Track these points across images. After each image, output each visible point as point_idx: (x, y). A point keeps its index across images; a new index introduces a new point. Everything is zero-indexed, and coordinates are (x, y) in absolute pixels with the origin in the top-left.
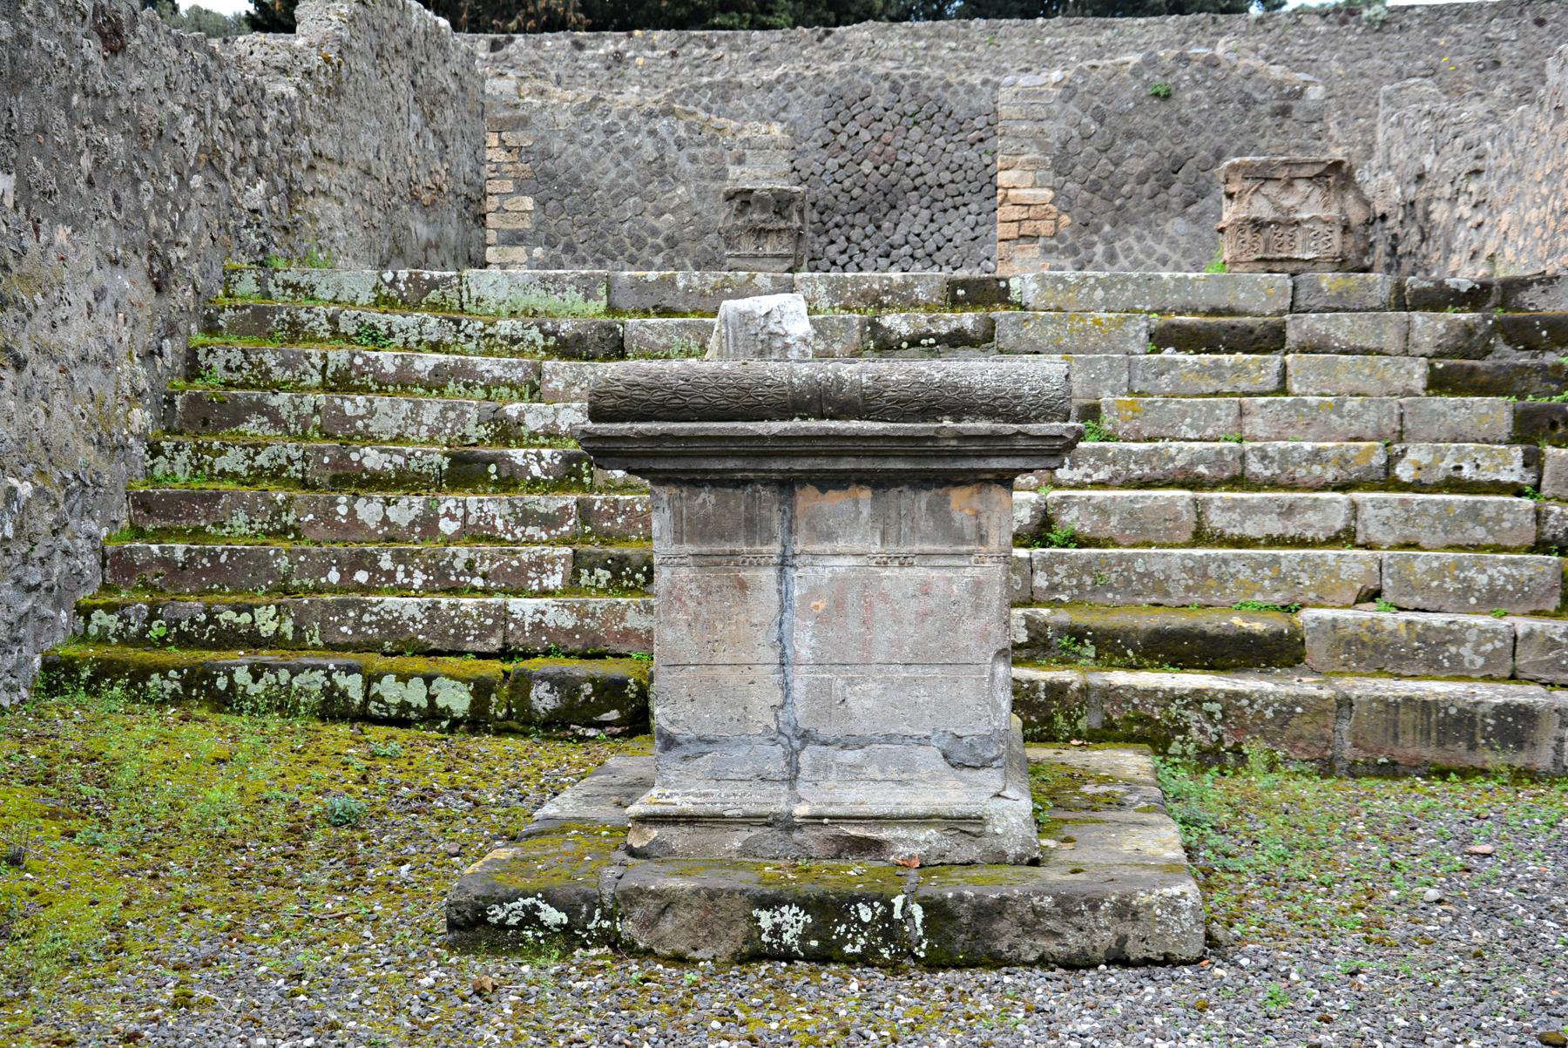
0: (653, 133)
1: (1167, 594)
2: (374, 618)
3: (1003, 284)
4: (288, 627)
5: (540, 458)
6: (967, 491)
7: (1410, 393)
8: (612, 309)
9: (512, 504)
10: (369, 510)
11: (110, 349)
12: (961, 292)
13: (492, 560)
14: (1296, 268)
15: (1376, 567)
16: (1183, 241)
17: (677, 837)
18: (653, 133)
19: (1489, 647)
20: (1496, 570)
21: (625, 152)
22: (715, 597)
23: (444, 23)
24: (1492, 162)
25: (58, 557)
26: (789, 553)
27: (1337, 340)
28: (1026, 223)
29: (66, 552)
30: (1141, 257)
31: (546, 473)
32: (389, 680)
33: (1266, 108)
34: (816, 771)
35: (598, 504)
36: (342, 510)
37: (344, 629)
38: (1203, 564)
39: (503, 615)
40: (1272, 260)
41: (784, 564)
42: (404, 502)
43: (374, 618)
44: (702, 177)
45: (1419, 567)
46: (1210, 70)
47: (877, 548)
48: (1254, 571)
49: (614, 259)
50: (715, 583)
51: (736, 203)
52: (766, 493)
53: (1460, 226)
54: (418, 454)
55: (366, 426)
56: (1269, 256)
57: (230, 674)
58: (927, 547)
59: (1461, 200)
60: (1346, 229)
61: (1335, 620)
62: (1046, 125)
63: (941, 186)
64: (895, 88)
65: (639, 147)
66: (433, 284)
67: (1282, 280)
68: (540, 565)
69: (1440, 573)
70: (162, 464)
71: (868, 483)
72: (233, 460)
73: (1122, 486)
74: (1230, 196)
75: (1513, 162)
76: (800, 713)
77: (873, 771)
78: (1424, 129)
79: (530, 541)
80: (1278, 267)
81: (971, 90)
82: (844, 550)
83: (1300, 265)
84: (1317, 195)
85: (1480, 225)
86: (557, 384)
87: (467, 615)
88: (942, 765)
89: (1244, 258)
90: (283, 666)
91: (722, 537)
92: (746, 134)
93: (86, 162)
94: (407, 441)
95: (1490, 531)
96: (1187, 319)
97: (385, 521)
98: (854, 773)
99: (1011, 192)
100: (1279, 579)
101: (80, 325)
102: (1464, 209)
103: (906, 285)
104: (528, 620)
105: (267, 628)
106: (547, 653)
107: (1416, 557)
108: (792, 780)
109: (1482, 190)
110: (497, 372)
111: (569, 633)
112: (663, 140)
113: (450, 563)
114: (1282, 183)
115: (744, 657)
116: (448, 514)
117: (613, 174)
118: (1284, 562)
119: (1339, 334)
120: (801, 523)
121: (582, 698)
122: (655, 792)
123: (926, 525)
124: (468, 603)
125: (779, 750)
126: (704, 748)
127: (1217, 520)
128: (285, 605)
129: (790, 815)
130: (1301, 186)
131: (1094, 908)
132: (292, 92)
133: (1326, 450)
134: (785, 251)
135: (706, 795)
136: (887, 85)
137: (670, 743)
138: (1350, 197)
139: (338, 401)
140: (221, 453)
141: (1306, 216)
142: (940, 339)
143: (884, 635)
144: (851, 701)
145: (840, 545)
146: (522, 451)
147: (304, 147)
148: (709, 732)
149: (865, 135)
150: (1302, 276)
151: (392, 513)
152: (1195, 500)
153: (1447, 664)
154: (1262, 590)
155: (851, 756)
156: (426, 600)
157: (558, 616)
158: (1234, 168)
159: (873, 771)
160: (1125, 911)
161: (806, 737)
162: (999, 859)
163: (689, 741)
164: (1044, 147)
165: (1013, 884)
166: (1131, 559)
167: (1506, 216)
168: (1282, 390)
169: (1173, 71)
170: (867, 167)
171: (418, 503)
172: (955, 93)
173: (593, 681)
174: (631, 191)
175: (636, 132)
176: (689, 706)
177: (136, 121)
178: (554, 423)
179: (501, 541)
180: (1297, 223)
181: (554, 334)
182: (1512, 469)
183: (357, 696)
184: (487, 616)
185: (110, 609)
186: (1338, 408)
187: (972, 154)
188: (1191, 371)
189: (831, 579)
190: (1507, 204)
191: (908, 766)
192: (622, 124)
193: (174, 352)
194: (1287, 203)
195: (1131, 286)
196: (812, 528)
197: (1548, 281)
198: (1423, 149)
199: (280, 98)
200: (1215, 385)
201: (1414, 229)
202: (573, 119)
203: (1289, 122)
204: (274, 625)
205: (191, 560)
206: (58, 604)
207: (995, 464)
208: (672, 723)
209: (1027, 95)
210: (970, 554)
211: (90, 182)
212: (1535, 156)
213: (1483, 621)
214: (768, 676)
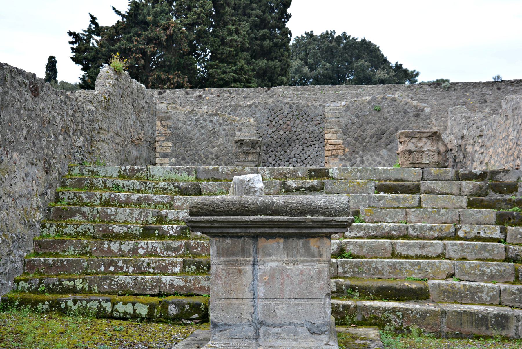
0: (211, 121)
1: (383, 275)
2: (116, 283)
3: (327, 171)
4: (86, 286)
5: (173, 228)
6: (315, 240)
7: (462, 208)
8: (197, 179)
9: (163, 244)
10: (115, 246)
11: (30, 193)
12: (313, 173)
13: (156, 263)
14: (423, 166)
15: (453, 266)
16: (386, 157)
18: (211, 121)
19: (491, 294)
20: (493, 268)
21: (202, 127)
22: (231, 275)
23: (143, 86)
24: (486, 133)
25: (9, 263)
26: (256, 260)
27: (437, 190)
28: (334, 151)
30: (372, 162)
31: (175, 233)
32: (120, 304)
33: (412, 114)
34: (265, 335)
35: (192, 243)
36: (106, 246)
37: (105, 287)
38: (395, 264)
39: (159, 281)
40: (415, 163)
41: (254, 264)
42: (127, 243)
43: (116, 283)
44: (227, 135)
45: (467, 266)
46: (393, 102)
47: (285, 259)
48: (412, 267)
49: (198, 162)
50: (231, 271)
51: (239, 144)
52: (248, 240)
53: (476, 153)
54: (132, 227)
55: (115, 218)
56: (414, 162)
57: (66, 303)
58: (302, 259)
59: (476, 145)
60: (439, 154)
61: (439, 284)
62: (340, 119)
63: (306, 138)
64: (291, 107)
65: (207, 126)
66: (138, 170)
67: (419, 170)
68: (172, 264)
69: (474, 268)
70: (45, 231)
71: (282, 237)
72: (69, 229)
73: (367, 238)
74: (401, 142)
75: (492, 133)
76: (260, 315)
77: (284, 335)
78: (463, 122)
79: (169, 256)
80: (417, 166)
81: (316, 108)
82: (274, 259)
83: (424, 165)
84: (429, 142)
85: (482, 153)
86: (179, 203)
87: (147, 281)
88: (308, 333)
89: (406, 163)
90: (84, 300)
91: (233, 255)
92: (242, 122)
93: (24, 132)
94: (128, 223)
95: (490, 254)
96: (388, 182)
97: (120, 250)
98: (278, 336)
99: (329, 141)
100: (420, 270)
101: (20, 185)
102: (477, 148)
103: (295, 171)
104: (168, 283)
105: (79, 286)
106: (174, 294)
107: (466, 263)
109: (483, 142)
110: (159, 199)
111: (182, 288)
112: (215, 123)
113: (142, 264)
114: (418, 139)
115: (241, 296)
116: (142, 247)
117: (198, 135)
118: (422, 264)
119: (438, 188)
120: (260, 250)
121: (186, 310)
122: (210, 343)
123: (302, 251)
124: (147, 277)
126: (227, 327)
127: (399, 250)
128: (85, 278)
130: (424, 140)
132: (93, 108)
133: (434, 226)
134: (255, 160)
135: (227, 344)
136: (288, 106)
137: (215, 326)
138: (440, 143)
139: (105, 209)
140: (65, 227)
141: (426, 149)
142: (306, 189)
145: (273, 258)
146: (167, 226)
147: (97, 126)
148: (229, 322)
149: (281, 122)
150: (425, 169)
151: (123, 247)
153: (478, 299)
154: (415, 273)
155: (277, 330)
158: (402, 134)
159: (284, 335)
161: (261, 324)
163: (222, 325)
164: (340, 126)
166: (371, 263)
167: (491, 150)
168: (420, 206)
169: (381, 102)
170: (282, 132)
171: (131, 243)
172: (310, 109)
173: (189, 304)
174: (204, 140)
175: (206, 121)
176: (222, 313)
177: (41, 118)
178: (177, 217)
179: (159, 256)
180: (423, 152)
181: (178, 187)
182: (497, 233)
183: (109, 310)
184: (154, 282)
185: (26, 280)
186: (438, 212)
187: (316, 128)
188: (389, 200)
189: (270, 269)
190: (491, 146)
191: (296, 334)
192: (201, 118)
193: (51, 193)
194: (419, 145)
195: (369, 172)
196: (264, 252)
197: (506, 171)
198: (463, 128)
199: (89, 110)
200: (397, 204)
201: (461, 154)
202: (185, 117)
203: (419, 119)
204: (81, 286)
205: (54, 263)
207: (325, 230)
208: (216, 319)
209: (334, 109)
210: (317, 261)
211: (25, 138)
212: (500, 131)
213: (489, 285)
214: (249, 302)
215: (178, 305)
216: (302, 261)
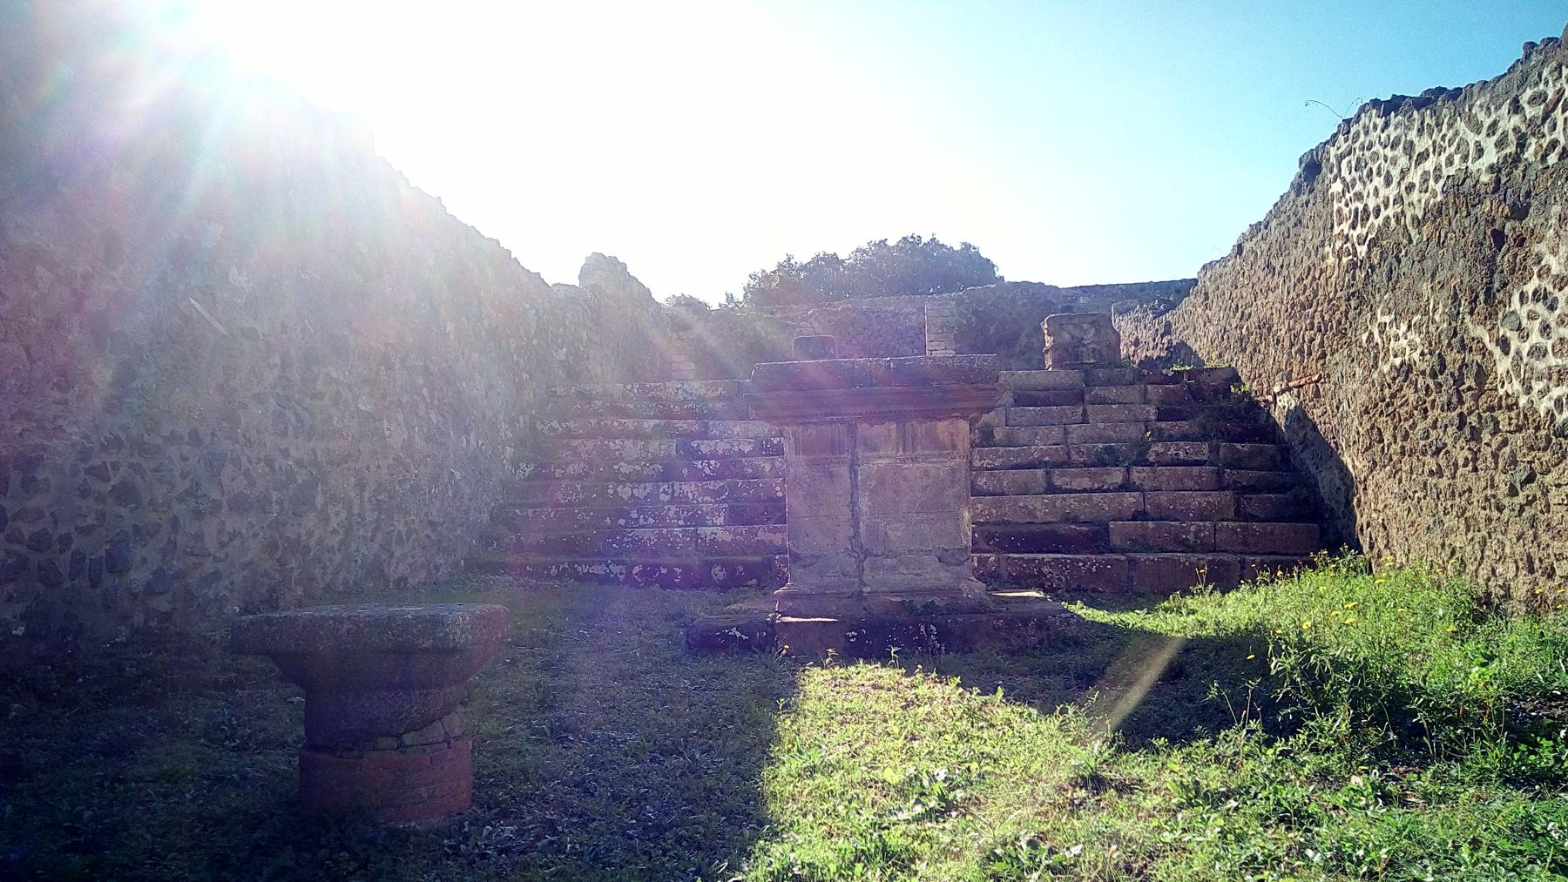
66: (651, 389)
88: (938, 565)
111: (729, 544)
127: (1058, 482)
161: (867, 553)
168: (1085, 421)
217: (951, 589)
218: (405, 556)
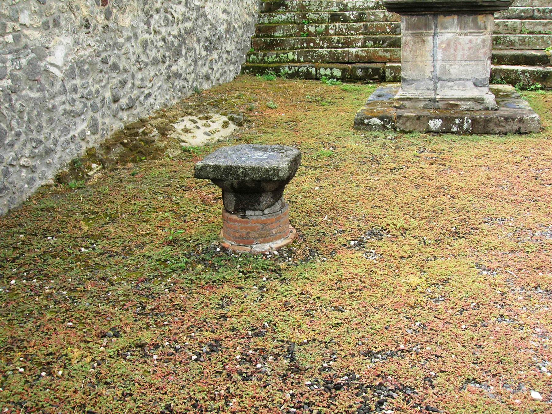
1: (515, 46)
4: (296, 57)
5: (353, 14)
6: (482, 16)
13: (344, 40)
17: (407, 104)
25: (243, 42)
29: (244, 41)
31: (354, 17)
34: (441, 87)
36: (306, 29)
38: (524, 38)
42: (320, 26)
47: (459, 31)
52: (430, 17)
58: (471, 31)
70: (261, 20)
79: (352, 34)
87: (339, 53)
88: (473, 86)
94: (319, 11)
106: (359, 62)
108: (435, 90)
111: (364, 57)
113: (333, 41)
115: (424, 59)
116: (331, 29)
118: (545, 38)
120: (439, 25)
123: (471, 25)
124: (339, 50)
125: (432, 82)
129: (435, 98)
131: (513, 120)
137: (404, 80)
143: (460, 54)
144: (451, 70)
145: (449, 30)
148: (415, 78)
152: (522, 23)
156: (329, 50)
157: (362, 53)
159: (456, 87)
160: (521, 120)
161: (439, 79)
162: (487, 109)
165: (492, 115)
166: (506, 37)
183: (314, 73)
185: (254, 54)
191: (465, 86)
196: (442, 26)
206: (243, 54)
207: (491, 9)
210: (482, 32)
214: (430, 64)
215: (362, 69)
216: (471, 33)
217: (479, 99)
218: (218, 69)
